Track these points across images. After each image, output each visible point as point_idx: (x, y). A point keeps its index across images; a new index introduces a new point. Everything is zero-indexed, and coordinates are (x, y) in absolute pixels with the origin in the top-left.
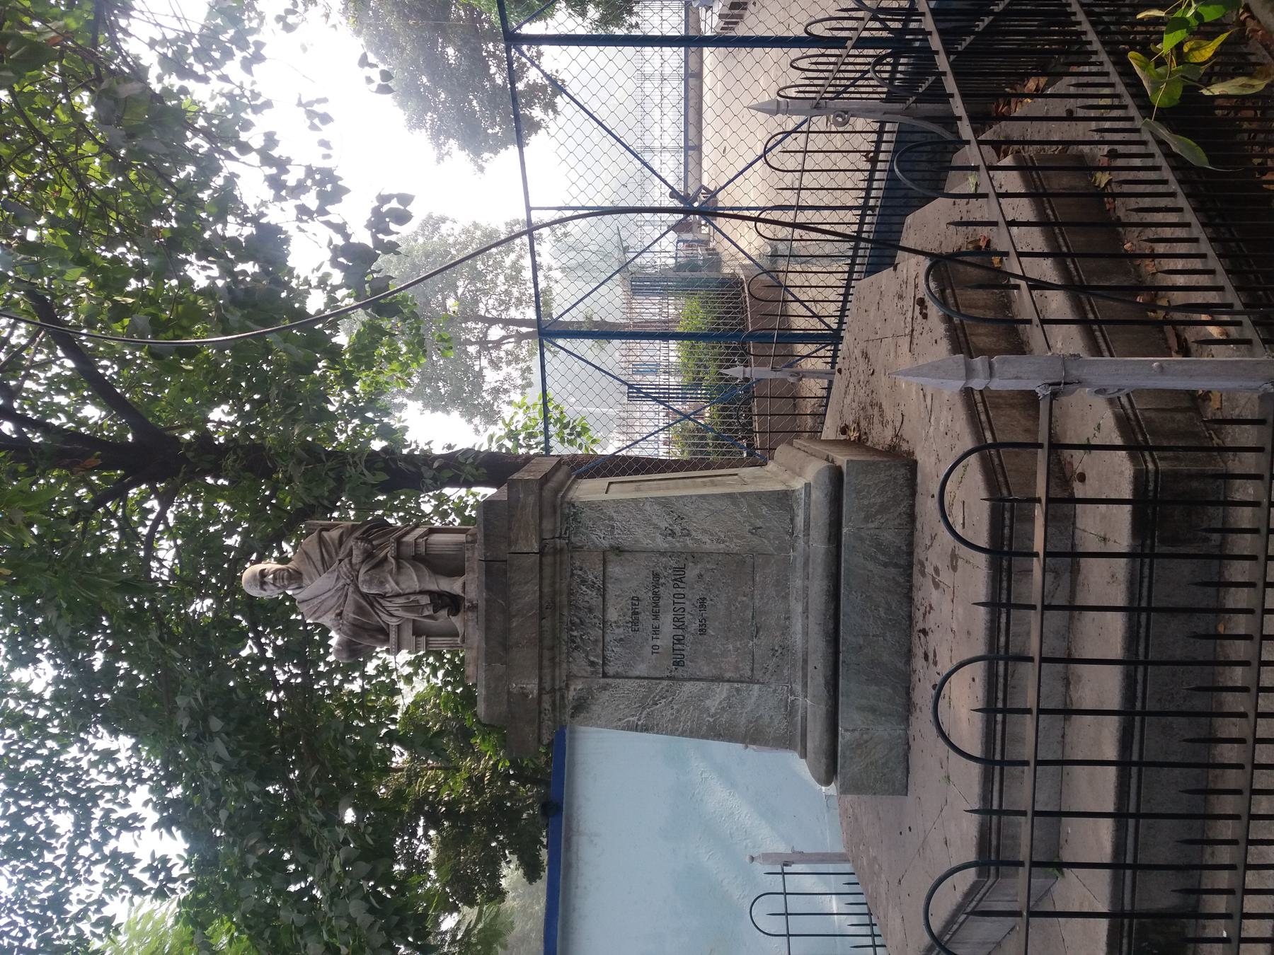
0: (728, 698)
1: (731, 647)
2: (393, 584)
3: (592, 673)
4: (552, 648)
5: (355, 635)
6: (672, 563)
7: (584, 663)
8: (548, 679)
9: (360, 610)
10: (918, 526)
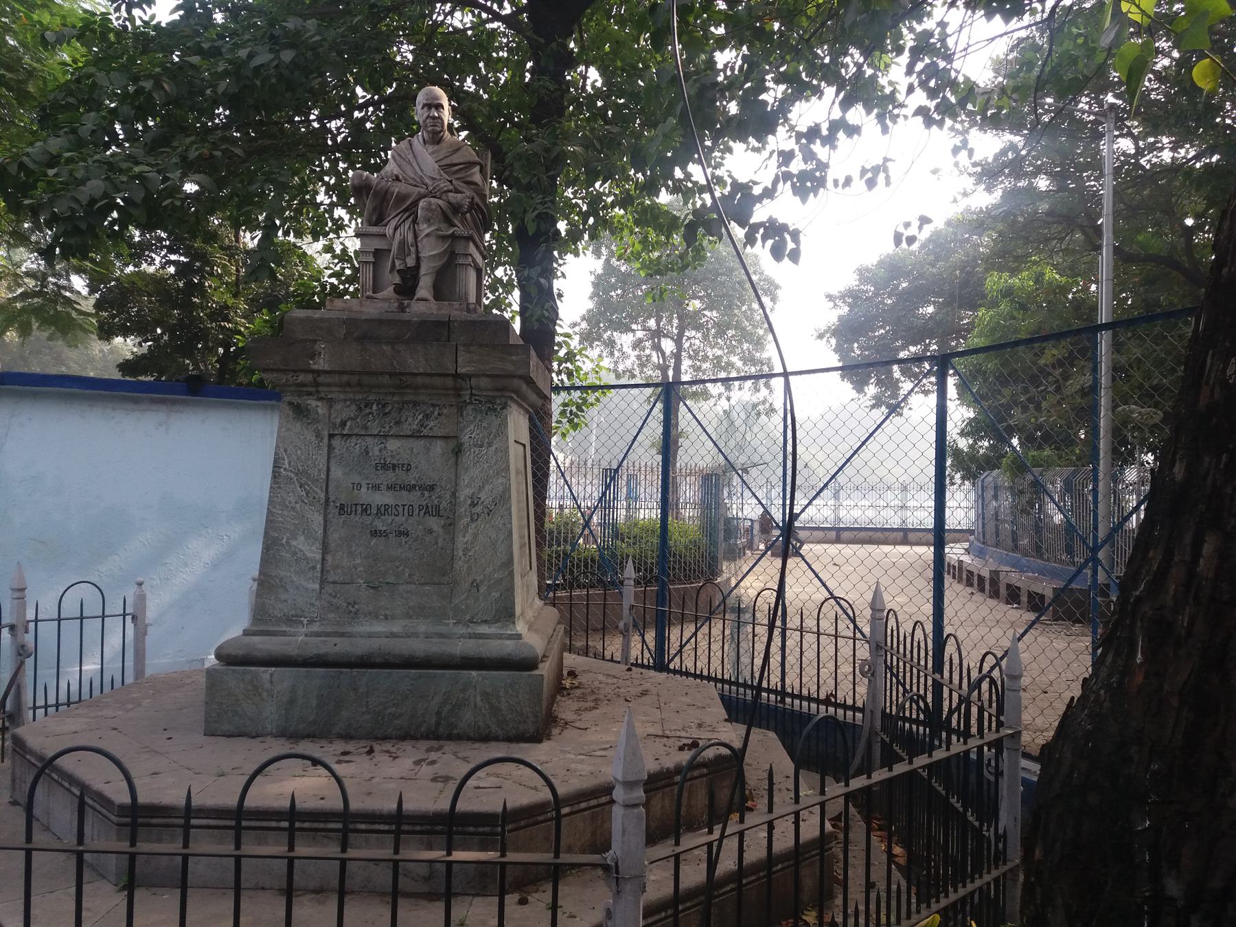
0: (306, 558)
1: (358, 561)
2: (427, 231)
3: (334, 424)
4: (360, 384)
5: (376, 193)
6: (444, 504)
7: (344, 416)
8: (329, 379)
9: (401, 198)
10: (477, 745)
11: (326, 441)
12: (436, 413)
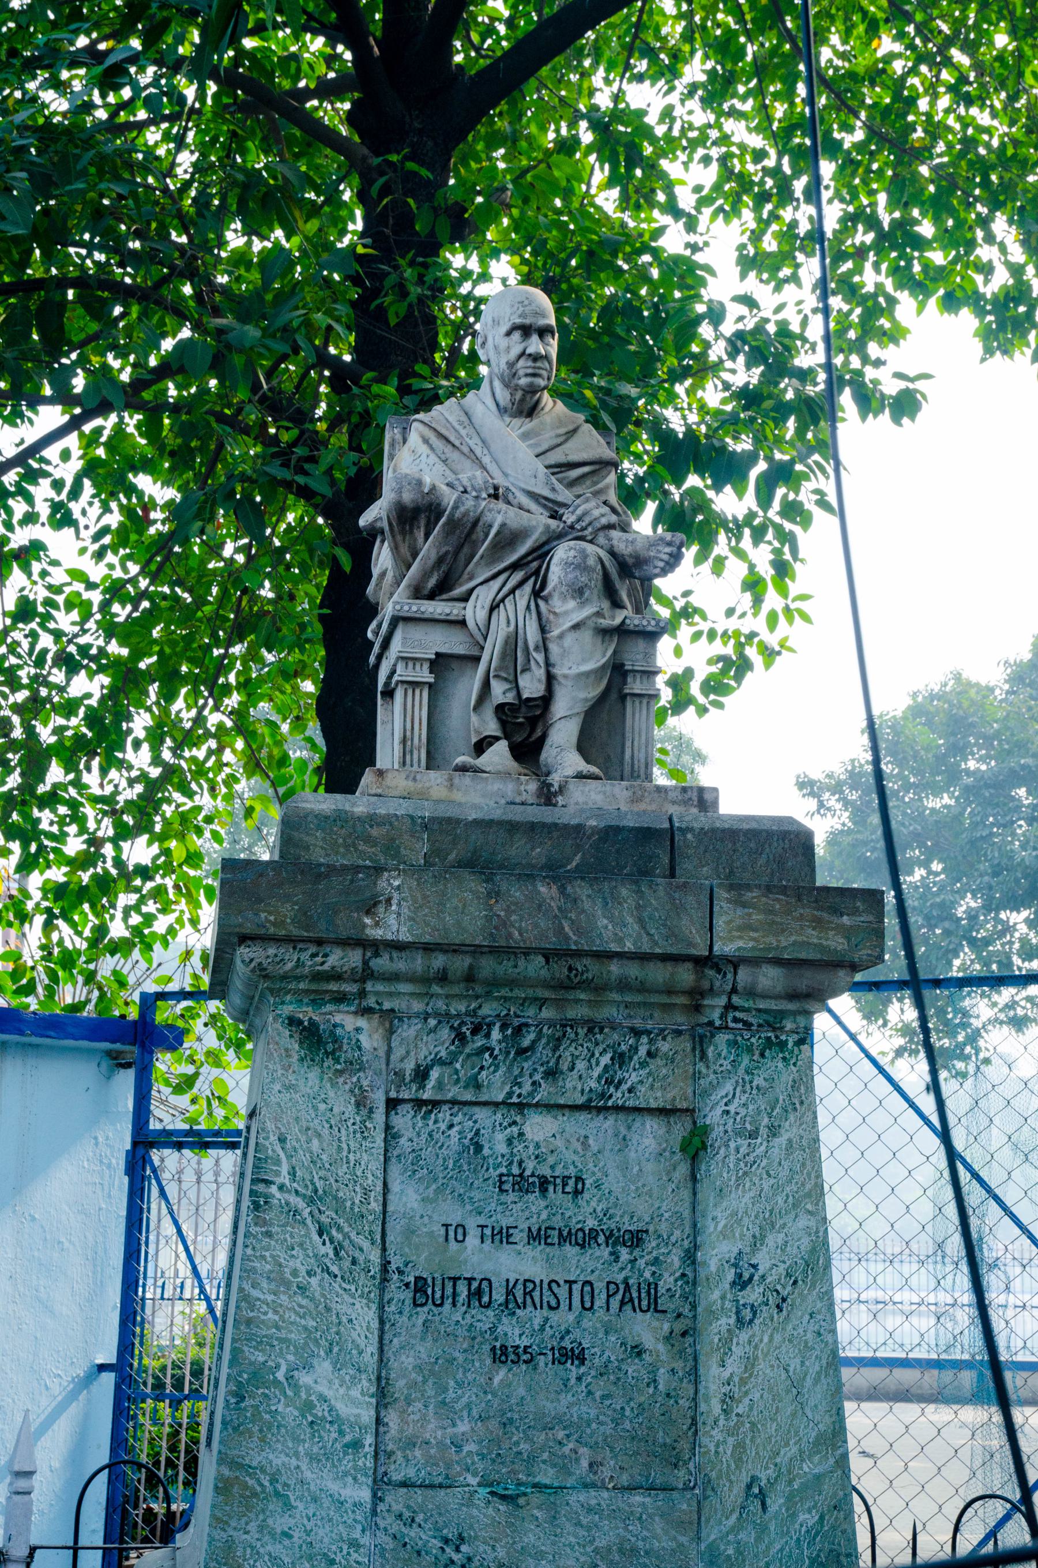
0: (336, 1420)
1: (463, 1427)
3: (399, 1074)
5: (453, 525)
6: (667, 1281)
7: (423, 1053)
8: (401, 964)
9: (508, 539)
11: (379, 1116)
12: (643, 1051)
